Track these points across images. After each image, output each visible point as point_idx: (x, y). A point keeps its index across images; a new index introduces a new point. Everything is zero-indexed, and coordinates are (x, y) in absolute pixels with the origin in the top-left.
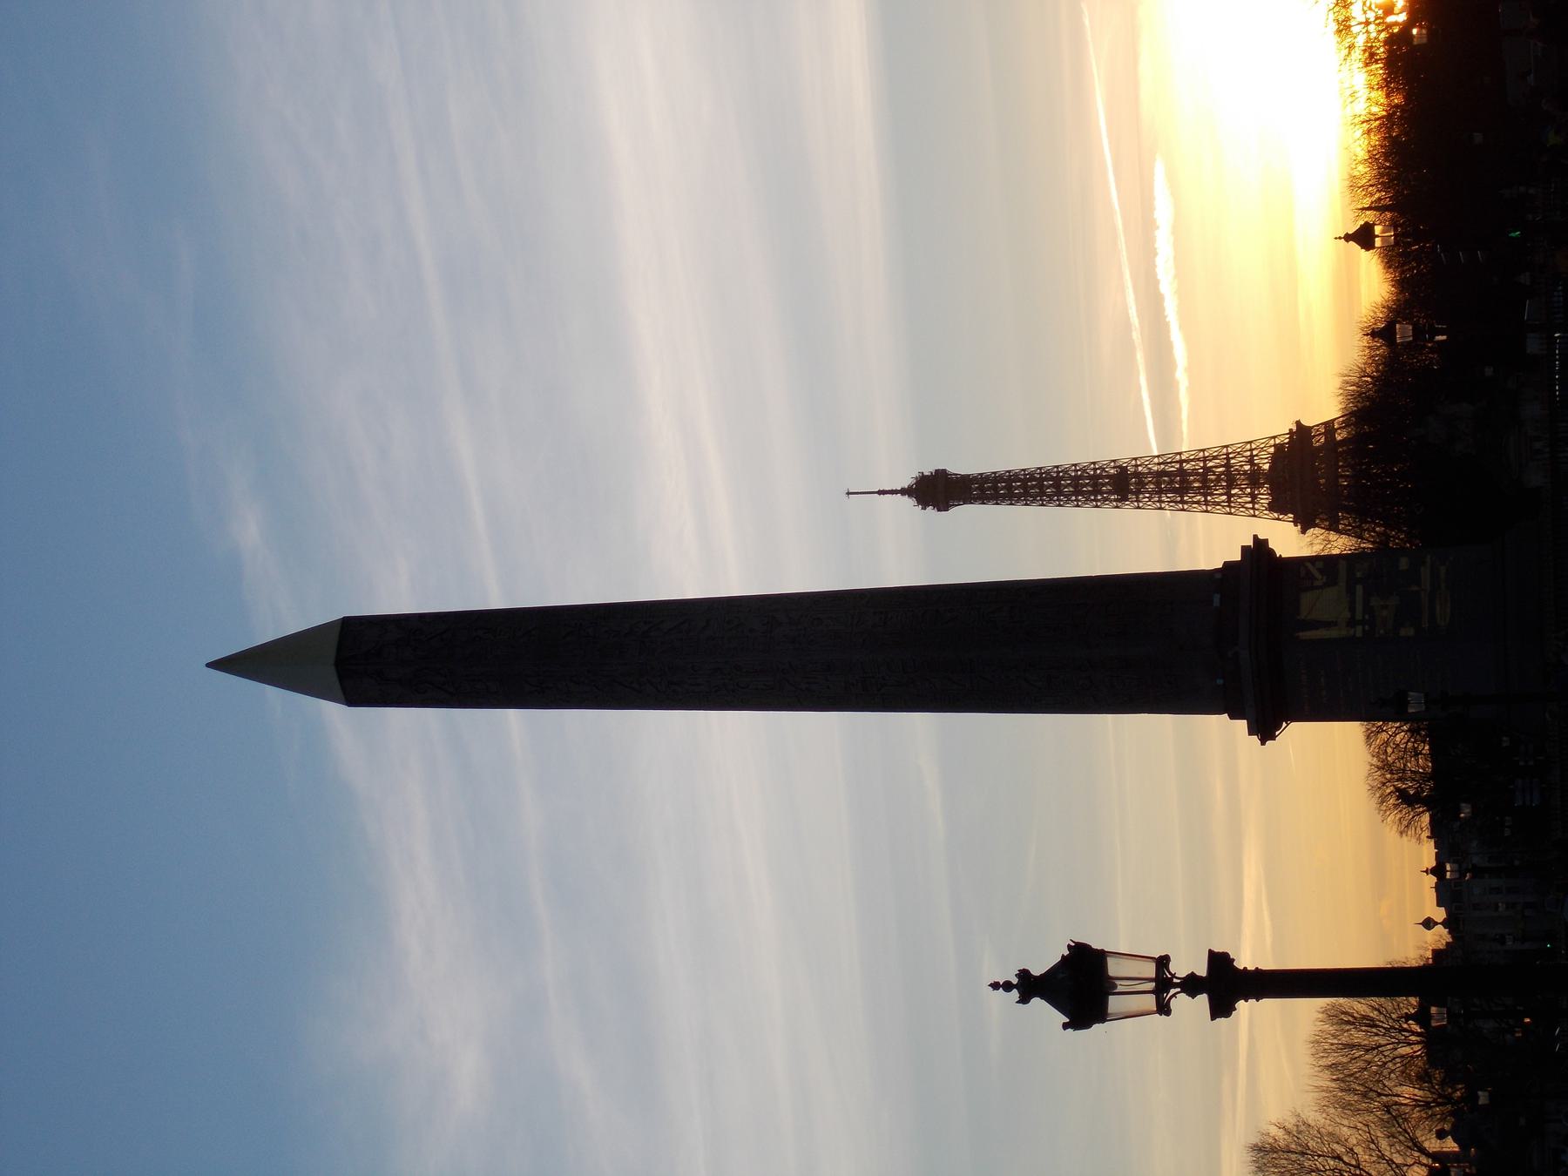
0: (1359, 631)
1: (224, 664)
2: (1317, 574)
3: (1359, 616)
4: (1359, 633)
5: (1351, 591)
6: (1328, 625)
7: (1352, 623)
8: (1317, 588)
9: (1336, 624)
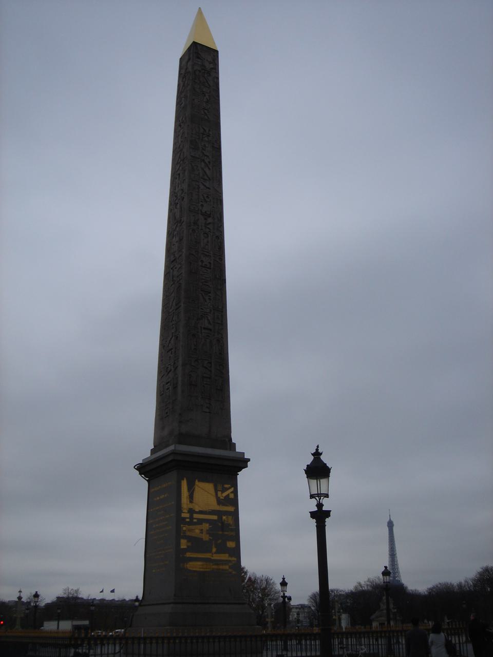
0: (185, 515)
1: (200, 12)
2: (225, 494)
3: (195, 516)
4: (183, 515)
5: (212, 512)
6: (191, 497)
7: (191, 511)
8: (216, 494)
9: (191, 502)
